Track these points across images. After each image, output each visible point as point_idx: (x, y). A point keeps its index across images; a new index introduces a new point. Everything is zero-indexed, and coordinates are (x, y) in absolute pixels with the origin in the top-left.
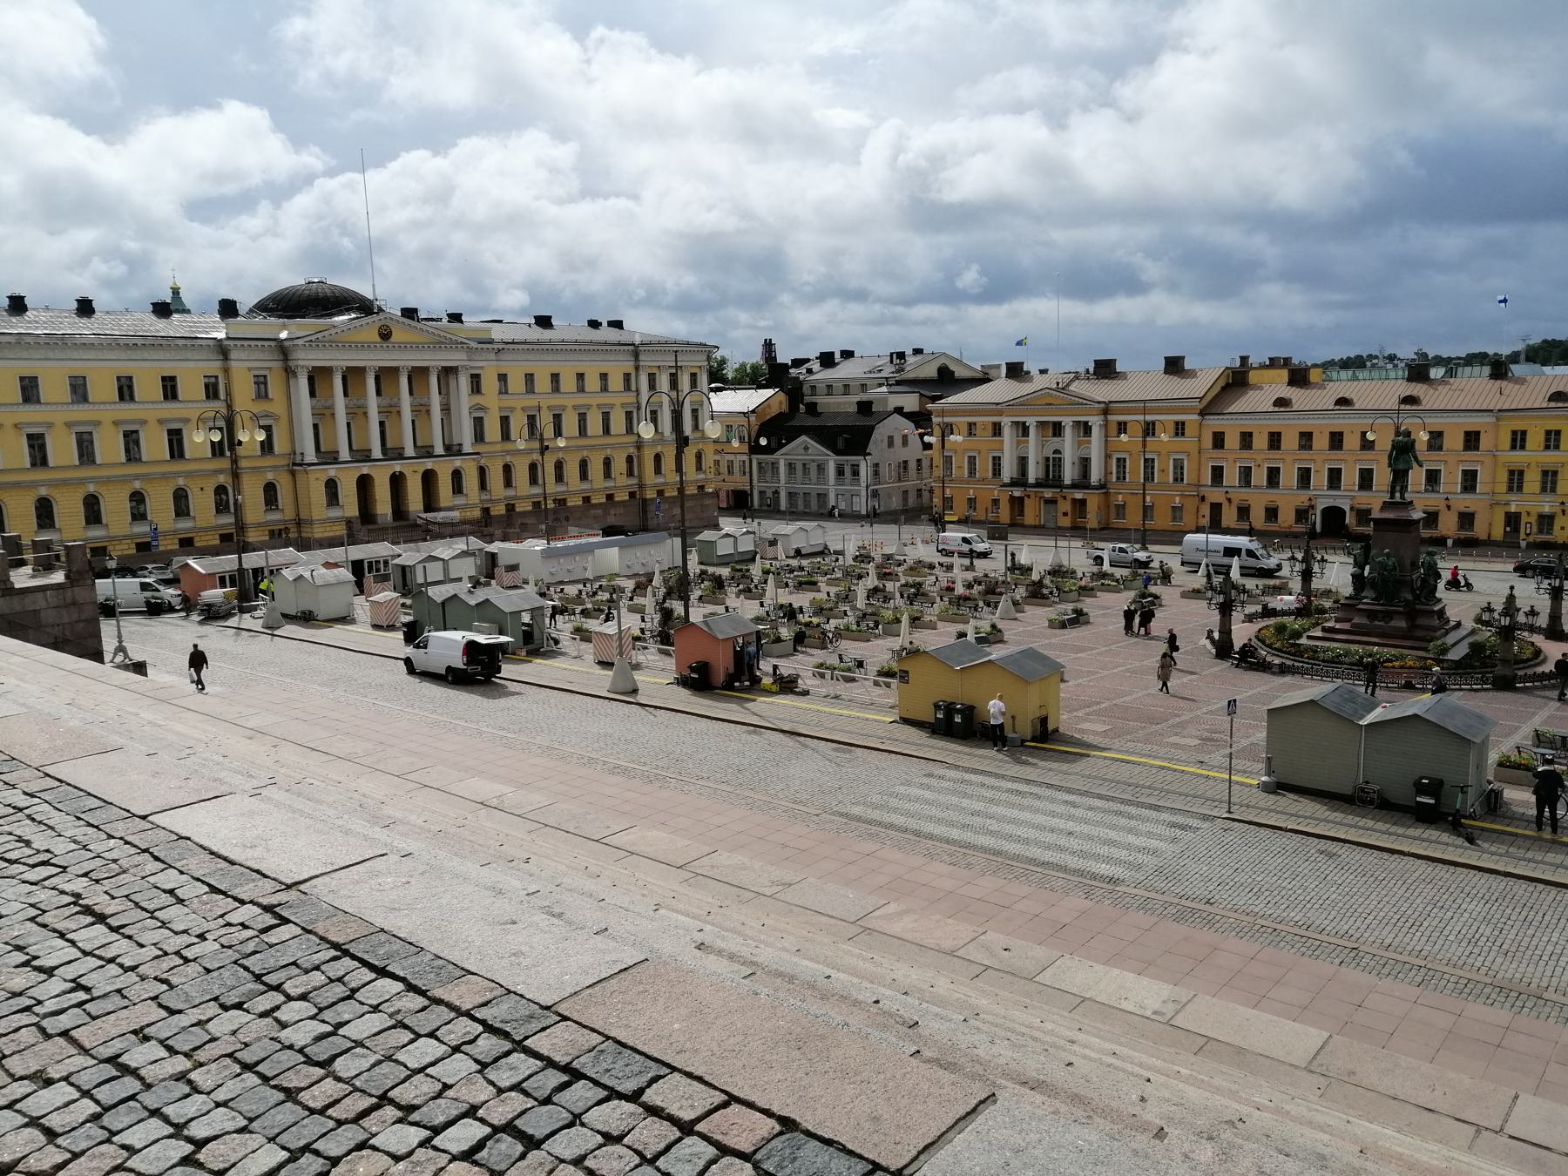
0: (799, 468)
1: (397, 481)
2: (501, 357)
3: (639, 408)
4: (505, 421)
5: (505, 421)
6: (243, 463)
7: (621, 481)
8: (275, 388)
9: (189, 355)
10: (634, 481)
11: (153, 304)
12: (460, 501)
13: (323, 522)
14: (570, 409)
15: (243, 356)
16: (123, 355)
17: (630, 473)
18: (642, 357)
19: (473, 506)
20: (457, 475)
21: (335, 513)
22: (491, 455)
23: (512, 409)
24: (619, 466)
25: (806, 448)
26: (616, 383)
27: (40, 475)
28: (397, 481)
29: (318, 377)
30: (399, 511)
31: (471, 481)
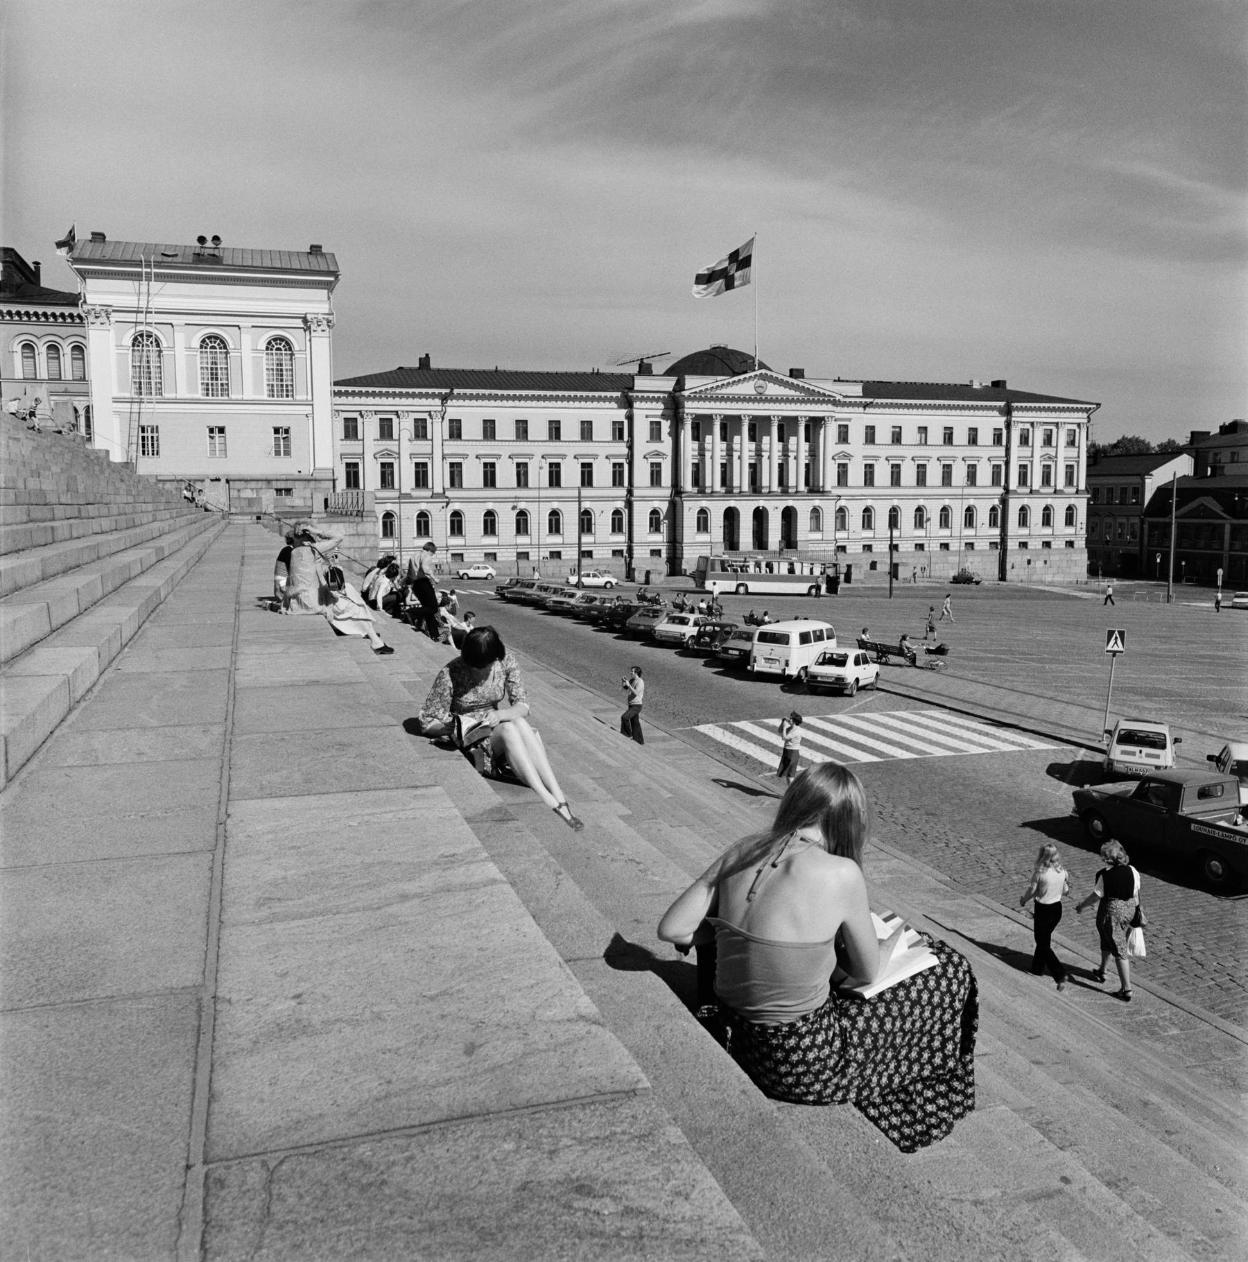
1: (760, 516)
2: (868, 410)
4: (869, 469)
5: (869, 469)
6: (636, 492)
12: (818, 536)
15: (643, 405)
17: (993, 523)
19: (828, 542)
20: (816, 512)
21: (703, 537)
22: (852, 498)
23: (876, 458)
27: (490, 493)
28: (760, 516)
29: (701, 426)
30: (760, 540)
31: (829, 519)
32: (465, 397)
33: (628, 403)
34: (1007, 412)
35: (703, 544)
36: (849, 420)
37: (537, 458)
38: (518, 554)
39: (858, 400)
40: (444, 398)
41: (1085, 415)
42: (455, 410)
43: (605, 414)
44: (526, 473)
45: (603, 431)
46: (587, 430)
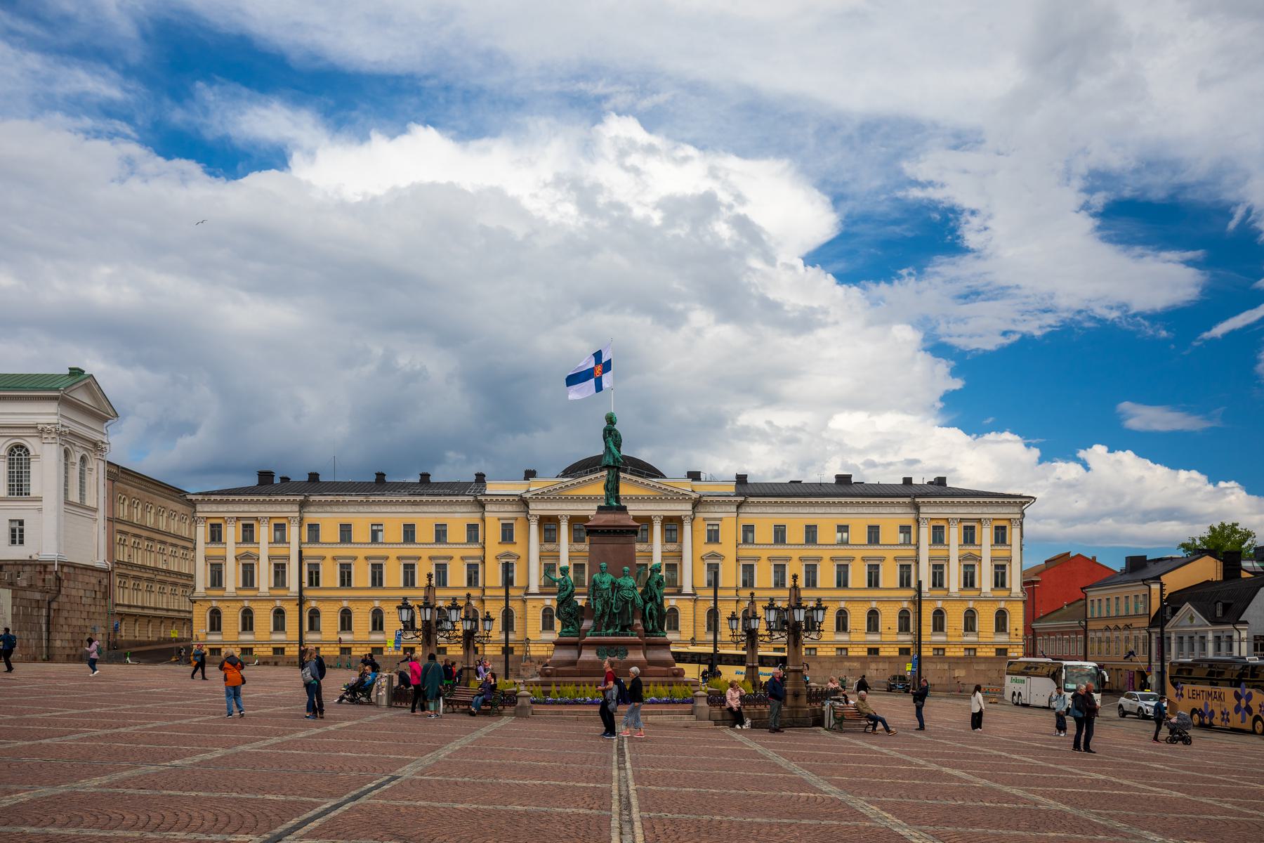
0: (1186, 639)
3: (917, 563)
6: (488, 592)
7: (890, 638)
8: (517, 534)
9: (458, 509)
10: (906, 638)
11: (310, 474)
13: (536, 642)
14: (764, 561)
15: (494, 508)
16: (410, 509)
17: (904, 628)
18: (923, 510)
24: (889, 618)
25: (1192, 618)
26: (889, 534)
32: (320, 503)
33: (482, 505)
34: (917, 507)
35: (545, 642)
36: (721, 519)
37: (425, 558)
38: (342, 649)
39: (733, 499)
40: (303, 505)
41: (1016, 510)
42: (312, 516)
43: (458, 519)
44: (381, 573)
45: (457, 533)
46: (441, 534)
